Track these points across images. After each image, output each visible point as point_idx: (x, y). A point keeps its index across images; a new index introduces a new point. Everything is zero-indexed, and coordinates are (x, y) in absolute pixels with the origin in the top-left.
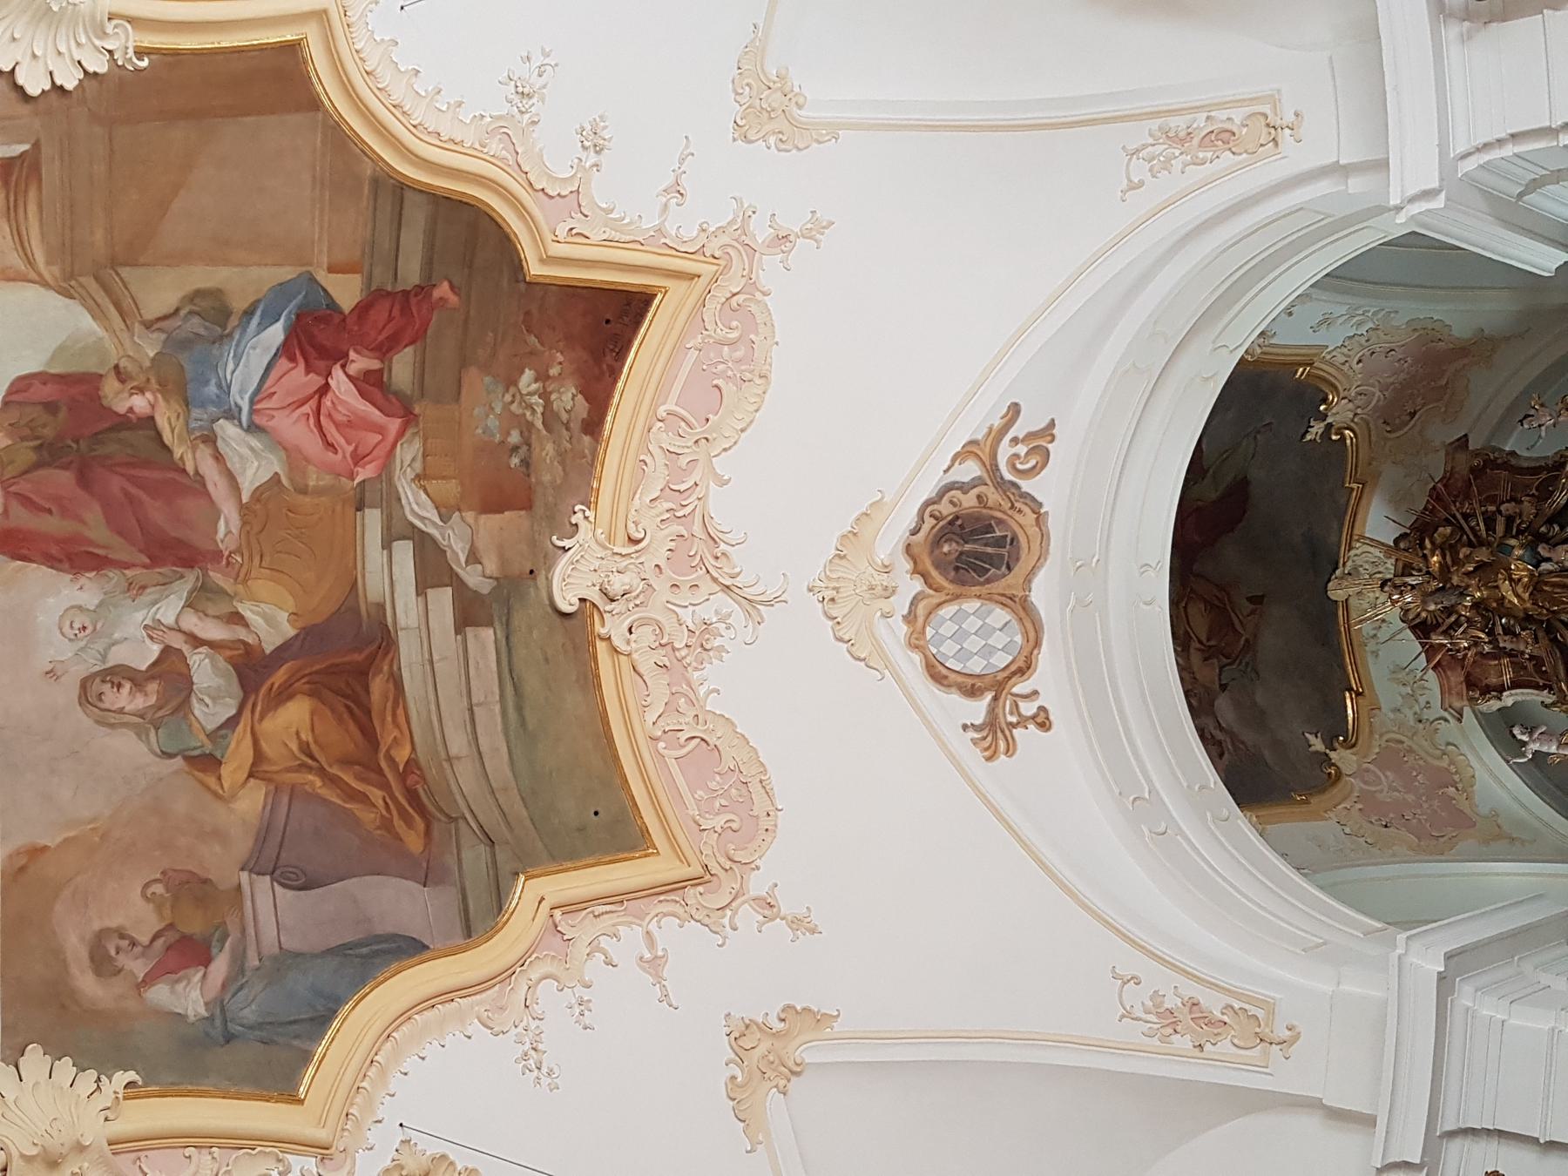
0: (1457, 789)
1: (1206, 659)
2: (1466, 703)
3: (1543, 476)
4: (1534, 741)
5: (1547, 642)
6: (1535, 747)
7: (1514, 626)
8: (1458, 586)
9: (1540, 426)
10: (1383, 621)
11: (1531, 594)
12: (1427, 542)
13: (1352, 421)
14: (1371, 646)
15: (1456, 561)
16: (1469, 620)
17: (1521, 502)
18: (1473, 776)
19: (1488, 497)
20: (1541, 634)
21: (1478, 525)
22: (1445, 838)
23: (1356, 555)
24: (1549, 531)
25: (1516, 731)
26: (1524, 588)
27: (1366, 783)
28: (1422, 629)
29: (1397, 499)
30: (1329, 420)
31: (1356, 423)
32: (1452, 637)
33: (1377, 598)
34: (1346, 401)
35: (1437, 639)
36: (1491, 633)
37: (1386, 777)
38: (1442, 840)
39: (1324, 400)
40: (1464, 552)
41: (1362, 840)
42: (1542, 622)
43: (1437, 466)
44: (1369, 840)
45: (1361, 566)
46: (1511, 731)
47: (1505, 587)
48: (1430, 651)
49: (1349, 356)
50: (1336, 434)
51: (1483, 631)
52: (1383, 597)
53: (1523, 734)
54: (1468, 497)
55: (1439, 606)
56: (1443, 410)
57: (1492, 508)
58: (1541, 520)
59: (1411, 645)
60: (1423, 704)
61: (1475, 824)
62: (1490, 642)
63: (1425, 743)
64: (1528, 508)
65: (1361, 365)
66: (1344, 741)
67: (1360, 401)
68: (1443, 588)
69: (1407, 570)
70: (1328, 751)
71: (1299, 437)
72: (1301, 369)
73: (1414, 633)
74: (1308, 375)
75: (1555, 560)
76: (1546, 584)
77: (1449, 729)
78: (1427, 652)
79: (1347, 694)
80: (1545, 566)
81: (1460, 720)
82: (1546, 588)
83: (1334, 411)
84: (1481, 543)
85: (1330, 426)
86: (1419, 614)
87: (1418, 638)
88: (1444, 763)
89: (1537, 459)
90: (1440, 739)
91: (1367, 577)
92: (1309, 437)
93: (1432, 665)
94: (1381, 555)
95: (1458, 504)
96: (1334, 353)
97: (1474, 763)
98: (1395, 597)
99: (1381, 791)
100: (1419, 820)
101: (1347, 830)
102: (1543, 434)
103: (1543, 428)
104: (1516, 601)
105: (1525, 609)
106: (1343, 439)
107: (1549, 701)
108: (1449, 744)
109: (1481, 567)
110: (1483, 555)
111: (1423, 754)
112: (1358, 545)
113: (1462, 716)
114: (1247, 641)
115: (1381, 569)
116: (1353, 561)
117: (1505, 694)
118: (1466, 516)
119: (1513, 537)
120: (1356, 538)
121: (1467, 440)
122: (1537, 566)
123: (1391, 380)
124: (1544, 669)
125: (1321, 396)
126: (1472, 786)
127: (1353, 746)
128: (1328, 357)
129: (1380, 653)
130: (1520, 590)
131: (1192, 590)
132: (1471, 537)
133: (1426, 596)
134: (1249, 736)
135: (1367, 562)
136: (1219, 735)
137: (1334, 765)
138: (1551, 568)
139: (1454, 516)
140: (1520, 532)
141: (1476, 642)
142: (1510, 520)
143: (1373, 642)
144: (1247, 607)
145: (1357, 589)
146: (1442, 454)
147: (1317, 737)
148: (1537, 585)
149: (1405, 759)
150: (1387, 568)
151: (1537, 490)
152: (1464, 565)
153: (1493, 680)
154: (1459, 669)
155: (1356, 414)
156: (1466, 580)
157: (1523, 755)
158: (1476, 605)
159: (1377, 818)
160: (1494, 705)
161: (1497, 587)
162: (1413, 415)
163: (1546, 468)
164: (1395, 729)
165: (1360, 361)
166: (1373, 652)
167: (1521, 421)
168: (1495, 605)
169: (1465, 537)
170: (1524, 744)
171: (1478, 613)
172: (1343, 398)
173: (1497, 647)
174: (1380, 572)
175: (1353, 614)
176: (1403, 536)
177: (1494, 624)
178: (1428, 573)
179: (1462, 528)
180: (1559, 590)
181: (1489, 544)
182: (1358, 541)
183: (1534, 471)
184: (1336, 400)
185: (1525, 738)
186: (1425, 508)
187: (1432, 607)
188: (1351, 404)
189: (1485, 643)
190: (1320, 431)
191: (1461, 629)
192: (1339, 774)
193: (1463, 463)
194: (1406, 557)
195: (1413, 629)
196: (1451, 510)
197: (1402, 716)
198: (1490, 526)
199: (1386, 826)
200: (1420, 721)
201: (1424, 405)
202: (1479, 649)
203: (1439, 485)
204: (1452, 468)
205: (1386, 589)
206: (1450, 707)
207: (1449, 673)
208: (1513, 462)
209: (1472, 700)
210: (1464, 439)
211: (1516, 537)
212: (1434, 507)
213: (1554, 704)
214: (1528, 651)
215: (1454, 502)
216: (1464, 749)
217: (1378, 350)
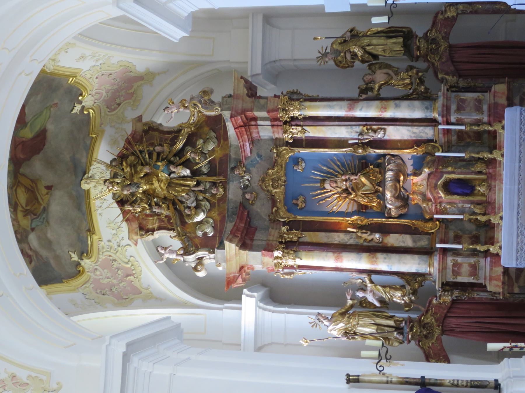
0: (135, 277)
1: (24, 216)
2: (139, 237)
3: (173, 135)
4: (167, 253)
5: (173, 209)
6: (167, 256)
7: (159, 202)
8: (137, 183)
9: (172, 112)
10: (105, 200)
11: (167, 187)
12: (124, 164)
13: (93, 105)
14: (99, 211)
15: (136, 172)
16: (141, 200)
17: (163, 146)
18: (141, 271)
19: (150, 143)
20: (171, 206)
21: (146, 155)
22: (129, 299)
23: (94, 168)
24: (175, 160)
25: (159, 249)
26: (164, 184)
27: (97, 275)
28: (121, 202)
29: (113, 142)
30: (83, 104)
31: (95, 106)
32: (133, 206)
33: (102, 189)
34: (90, 96)
35: (128, 208)
36: (150, 205)
37: (105, 272)
38: (127, 300)
39: (81, 95)
40: (139, 168)
41: (93, 301)
42: (171, 200)
43: (129, 129)
44: (97, 301)
45: (96, 174)
46: (157, 249)
47: (156, 184)
48: (125, 213)
49: (92, 75)
50: (86, 111)
51: (147, 204)
52: (105, 188)
53: (162, 250)
54: (141, 143)
55: (129, 192)
56: (132, 104)
57: (151, 148)
58: (170, 156)
59: (116, 210)
60: (121, 239)
61: (141, 293)
62: (149, 209)
63: (122, 256)
64: (166, 148)
65: (97, 79)
66: (87, 254)
67: (97, 96)
68: (130, 184)
69: (115, 176)
70: (79, 261)
71: (70, 111)
72: (71, 79)
73: (118, 205)
74: (75, 82)
75: (177, 172)
76: (173, 183)
77: (131, 250)
78: (123, 213)
79: (89, 233)
80: (172, 175)
81: (136, 244)
82: (173, 185)
83: (85, 100)
84: (147, 164)
85: (83, 107)
86: (119, 196)
87: (119, 206)
88: (129, 266)
89: (171, 128)
90: (128, 254)
91: (98, 178)
92: (74, 111)
93: (125, 220)
94: (105, 168)
95: (137, 146)
96: (86, 73)
97: (142, 264)
98: (110, 188)
99: (102, 279)
100: (118, 292)
101: (87, 297)
102: (173, 116)
103: (173, 113)
104: (160, 190)
105: (164, 194)
106: (89, 113)
107: (173, 236)
108: (131, 256)
109: (146, 175)
110: (147, 170)
111: (120, 262)
112: (95, 163)
113: (137, 243)
114: (44, 207)
115: (104, 175)
116: (93, 171)
117: (155, 232)
118: (141, 152)
119: (160, 162)
120: (94, 160)
121: (142, 118)
122: (169, 175)
123: (110, 88)
124: (171, 221)
125: (79, 93)
126: (140, 276)
127: (90, 258)
128: (83, 75)
129: (103, 214)
130: (162, 185)
131: (19, 182)
132: (143, 161)
133: (123, 187)
134: (44, 253)
135: (98, 172)
136: (30, 253)
137: (82, 267)
138: (175, 176)
139: (136, 152)
140: (163, 160)
141: (144, 209)
142: (159, 154)
143: (101, 209)
144: (44, 191)
145: (94, 184)
146: (131, 123)
147: (74, 253)
148: (170, 184)
149: (113, 264)
150: (107, 175)
151: (170, 141)
152: (139, 174)
153: (150, 226)
154: (136, 222)
155: (95, 102)
156: (140, 180)
157: (162, 260)
158: (144, 192)
159: (100, 291)
160: (150, 238)
161: (152, 184)
162: (119, 105)
163: (175, 132)
164: (109, 250)
165: (97, 78)
166: (100, 214)
167: (164, 110)
168: (152, 192)
169: (140, 161)
170: (163, 254)
171: (144, 195)
172: (90, 94)
173: (152, 211)
174: (104, 177)
175: (92, 196)
176: (114, 160)
177: (151, 201)
178: (124, 177)
179: (138, 157)
180: (178, 186)
181: (150, 165)
182: (95, 161)
183: (169, 133)
184: (86, 95)
185: (163, 252)
186: (124, 147)
187: (125, 192)
188: (93, 97)
189: (147, 209)
190: (79, 109)
191: (138, 203)
192: (84, 271)
193: (140, 127)
194: (116, 170)
195: (118, 202)
196: (134, 148)
197: (111, 244)
198: (150, 155)
199: (104, 294)
200: (119, 246)
201: (124, 101)
202: (145, 212)
203: (130, 137)
204: (135, 130)
205: (106, 184)
206: (132, 239)
207: (132, 223)
208: (161, 128)
209: (142, 236)
210: (141, 117)
211: (161, 162)
212: (127, 147)
213: (175, 237)
214: (165, 213)
215: (136, 145)
216: (138, 259)
217: (105, 73)
